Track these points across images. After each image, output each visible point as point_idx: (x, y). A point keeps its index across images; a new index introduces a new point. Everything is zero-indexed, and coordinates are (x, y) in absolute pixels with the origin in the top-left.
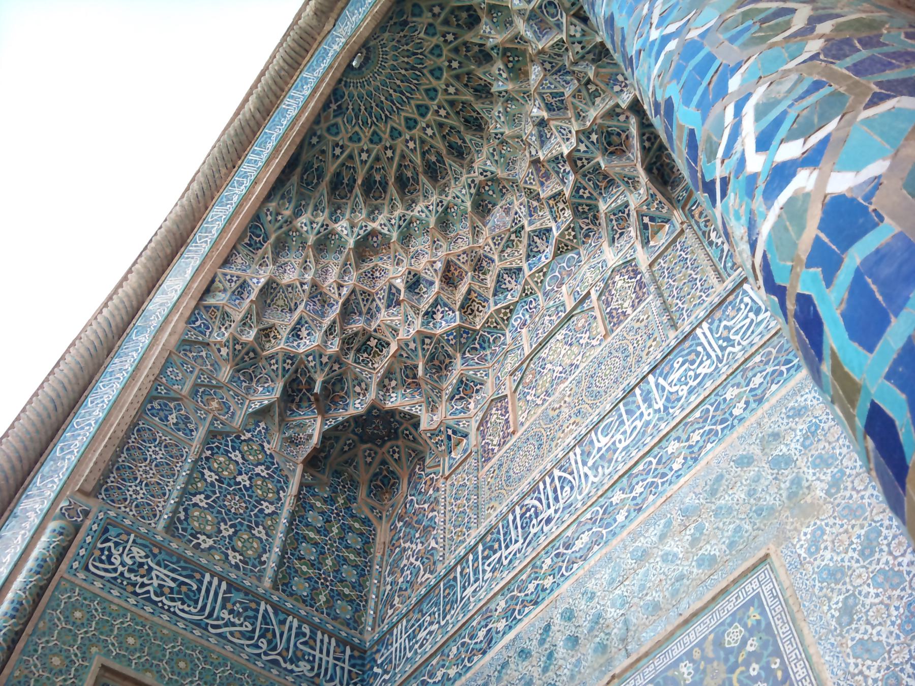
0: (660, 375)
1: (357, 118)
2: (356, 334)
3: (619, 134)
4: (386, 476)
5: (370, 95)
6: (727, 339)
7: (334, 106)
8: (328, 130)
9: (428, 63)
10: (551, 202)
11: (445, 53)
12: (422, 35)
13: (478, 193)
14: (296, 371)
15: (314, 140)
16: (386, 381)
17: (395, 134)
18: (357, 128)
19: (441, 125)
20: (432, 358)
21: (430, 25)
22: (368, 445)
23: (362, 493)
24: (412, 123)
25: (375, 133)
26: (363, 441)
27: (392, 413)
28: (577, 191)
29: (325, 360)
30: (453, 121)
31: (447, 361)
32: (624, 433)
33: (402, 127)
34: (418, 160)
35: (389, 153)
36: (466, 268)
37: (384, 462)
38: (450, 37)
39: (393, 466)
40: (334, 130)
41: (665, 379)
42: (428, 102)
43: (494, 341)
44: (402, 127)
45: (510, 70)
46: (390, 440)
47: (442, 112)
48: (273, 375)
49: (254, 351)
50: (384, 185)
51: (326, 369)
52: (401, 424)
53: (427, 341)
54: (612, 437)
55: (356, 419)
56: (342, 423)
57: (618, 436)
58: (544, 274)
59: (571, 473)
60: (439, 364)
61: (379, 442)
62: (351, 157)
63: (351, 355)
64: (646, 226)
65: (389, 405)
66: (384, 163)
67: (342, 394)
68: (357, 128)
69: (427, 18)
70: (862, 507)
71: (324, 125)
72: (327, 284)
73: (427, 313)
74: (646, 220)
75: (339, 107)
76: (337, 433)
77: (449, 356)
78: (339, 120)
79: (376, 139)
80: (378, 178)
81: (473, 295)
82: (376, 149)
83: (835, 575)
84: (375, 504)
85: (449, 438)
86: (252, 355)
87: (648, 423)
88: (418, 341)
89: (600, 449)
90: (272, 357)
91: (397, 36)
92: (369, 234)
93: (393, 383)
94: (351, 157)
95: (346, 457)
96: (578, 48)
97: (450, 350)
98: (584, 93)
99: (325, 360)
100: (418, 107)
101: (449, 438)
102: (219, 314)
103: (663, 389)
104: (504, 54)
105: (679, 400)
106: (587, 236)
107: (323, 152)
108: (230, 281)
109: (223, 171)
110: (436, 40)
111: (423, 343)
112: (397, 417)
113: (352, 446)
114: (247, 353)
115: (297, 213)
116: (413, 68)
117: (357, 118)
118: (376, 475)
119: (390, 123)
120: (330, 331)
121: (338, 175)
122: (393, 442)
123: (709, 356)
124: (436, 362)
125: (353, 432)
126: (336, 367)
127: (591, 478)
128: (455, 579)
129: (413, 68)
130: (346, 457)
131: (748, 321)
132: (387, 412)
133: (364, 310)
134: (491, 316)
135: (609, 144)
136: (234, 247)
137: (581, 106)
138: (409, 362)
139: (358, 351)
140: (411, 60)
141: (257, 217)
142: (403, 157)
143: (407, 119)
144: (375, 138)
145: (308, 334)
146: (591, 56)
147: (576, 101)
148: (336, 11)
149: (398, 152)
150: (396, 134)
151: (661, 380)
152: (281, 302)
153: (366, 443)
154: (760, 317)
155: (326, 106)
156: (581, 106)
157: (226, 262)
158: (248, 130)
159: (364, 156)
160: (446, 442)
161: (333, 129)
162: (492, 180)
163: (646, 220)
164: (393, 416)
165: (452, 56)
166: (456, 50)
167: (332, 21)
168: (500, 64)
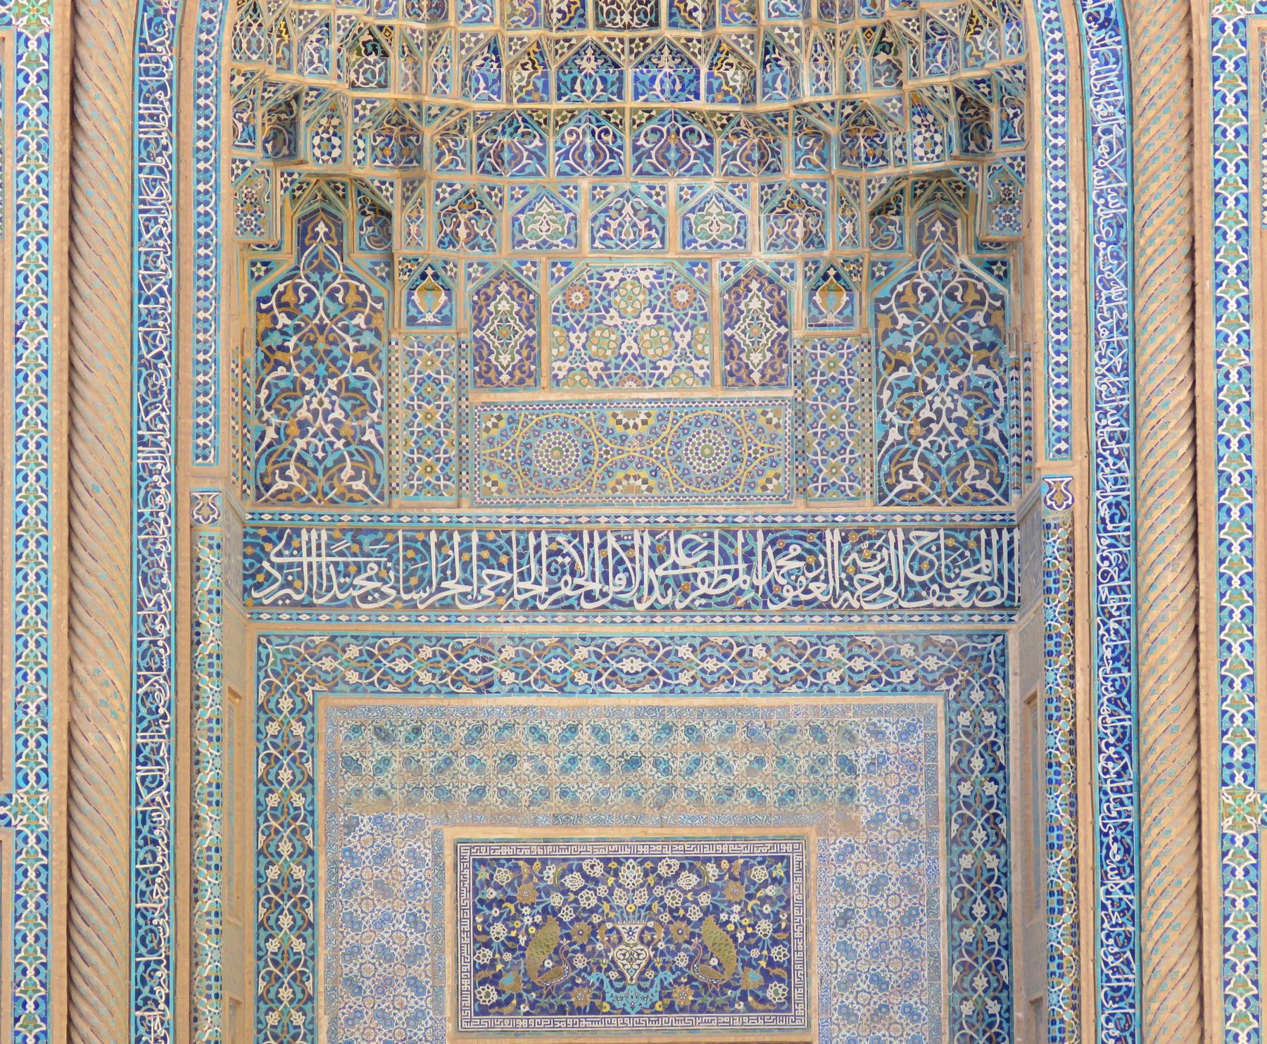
0: (773, 543)
6: (850, 578)
32: (711, 575)
41: (776, 553)
43: (523, 135)
48: (258, 102)
54: (695, 565)
57: (701, 572)
58: (649, 118)
59: (632, 560)
64: (826, 277)
65: (358, 171)
70: (885, 855)
74: (832, 272)
83: (846, 886)
85: (424, 276)
87: (740, 592)
89: (675, 566)
103: (769, 568)
105: (782, 599)
106: (736, 135)
123: (826, 581)
127: (656, 594)
131: (876, 581)
137: (862, 46)
145: (318, 40)
147: (861, 36)
151: (770, 551)
154: (888, 591)
156: (862, 46)
163: (832, 272)
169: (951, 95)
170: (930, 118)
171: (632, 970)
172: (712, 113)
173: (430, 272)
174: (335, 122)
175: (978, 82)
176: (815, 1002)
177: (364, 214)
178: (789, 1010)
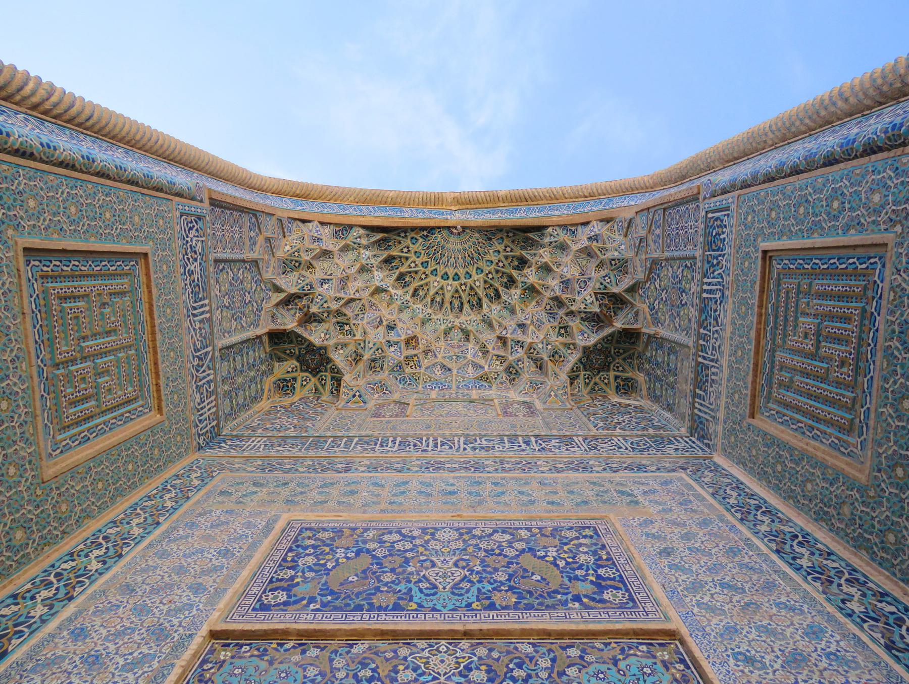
1: (428, 248)
2: (345, 315)
3: (560, 357)
4: (288, 386)
5: (443, 247)
7: (425, 233)
8: (412, 238)
9: (480, 263)
10: (495, 358)
11: (492, 267)
12: (491, 251)
13: (450, 329)
14: (306, 295)
15: (403, 235)
16: (339, 347)
17: (434, 272)
18: (423, 252)
19: (457, 291)
20: (373, 361)
21: (499, 252)
22: (298, 364)
23: (272, 379)
24: (445, 277)
25: (427, 262)
26: (298, 360)
27: (329, 360)
28: (518, 361)
29: (325, 305)
30: (465, 297)
31: (378, 369)
33: (440, 273)
34: (432, 292)
35: (423, 276)
36: (421, 346)
37: (295, 379)
38: (501, 264)
39: (297, 385)
40: (414, 241)
42: (462, 277)
44: (440, 273)
45: (521, 298)
46: (310, 373)
47: (463, 287)
48: (295, 283)
49: (300, 264)
50: (406, 285)
51: (321, 310)
52: (326, 371)
53: (380, 351)
55: (311, 344)
56: (303, 338)
60: (375, 364)
61: (304, 368)
62: (407, 258)
63: (335, 320)
64: (550, 396)
65: (331, 356)
66: (417, 277)
67: (313, 329)
68: (423, 252)
69: (501, 248)
71: (413, 234)
72: (355, 283)
73: (389, 342)
74: (553, 393)
75: (427, 236)
76: (294, 340)
77: (382, 368)
78: (421, 240)
79: (425, 265)
80: (407, 279)
81: (416, 358)
82: (420, 268)
84: (272, 389)
85: (354, 396)
86: (297, 264)
88: (376, 347)
90: (304, 277)
91: (480, 240)
92: (386, 291)
93: (341, 352)
94: (407, 258)
95: (283, 355)
96: (583, 306)
97: (385, 366)
98: (557, 330)
99: (325, 305)
100: (456, 274)
101: (354, 396)
102: (300, 234)
104: (525, 289)
107: (400, 243)
108: (317, 231)
109: (352, 198)
110: (495, 259)
111: (378, 350)
112: (329, 366)
113: (291, 355)
114: (296, 261)
115: (366, 247)
116: (472, 258)
117: (428, 248)
118: (285, 380)
119: (437, 267)
120: (338, 299)
121: (394, 258)
122: (310, 376)
124: (373, 365)
125: (300, 350)
126: (326, 315)
128: (326, 442)
129: (472, 258)
130: (283, 355)
132: (328, 358)
133: (356, 313)
134: (419, 373)
135: (553, 356)
136: (330, 224)
137: (552, 333)
138: (360, 351)
139: (338, 323)
140: (475, 255)
141: (351, 227)
142: (426, 284)
143: (446, 273)
144: (425, 264)
146: (583, 315)
147: (551, 330)
148: (464, 207)
149: (427, 280)
150: (435, 273)
152: (325, 266)
153: (298, 361)
155: (423, 229)
157: (322, 223)
158: (379, 199)
159: (413, 265)
160: (350, 396)
161: (414, 240)
162: (462, 330)
164: (327, 363)
165: (494, 272)
166: (497, 271)
167: (457, 208)
168: (518, 292)
169: (594, 298)
170: (586, 335)
171: (445, 586)
172: (491, 372)
173: (357, 394)
174: (327, 337)
175: (604, 277)
176: (665, 601)
177: (332, 393)
178: (635, 606)
